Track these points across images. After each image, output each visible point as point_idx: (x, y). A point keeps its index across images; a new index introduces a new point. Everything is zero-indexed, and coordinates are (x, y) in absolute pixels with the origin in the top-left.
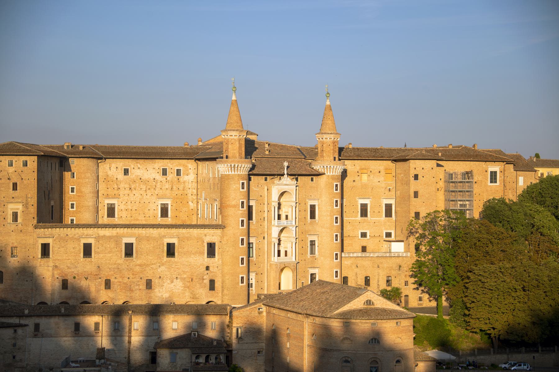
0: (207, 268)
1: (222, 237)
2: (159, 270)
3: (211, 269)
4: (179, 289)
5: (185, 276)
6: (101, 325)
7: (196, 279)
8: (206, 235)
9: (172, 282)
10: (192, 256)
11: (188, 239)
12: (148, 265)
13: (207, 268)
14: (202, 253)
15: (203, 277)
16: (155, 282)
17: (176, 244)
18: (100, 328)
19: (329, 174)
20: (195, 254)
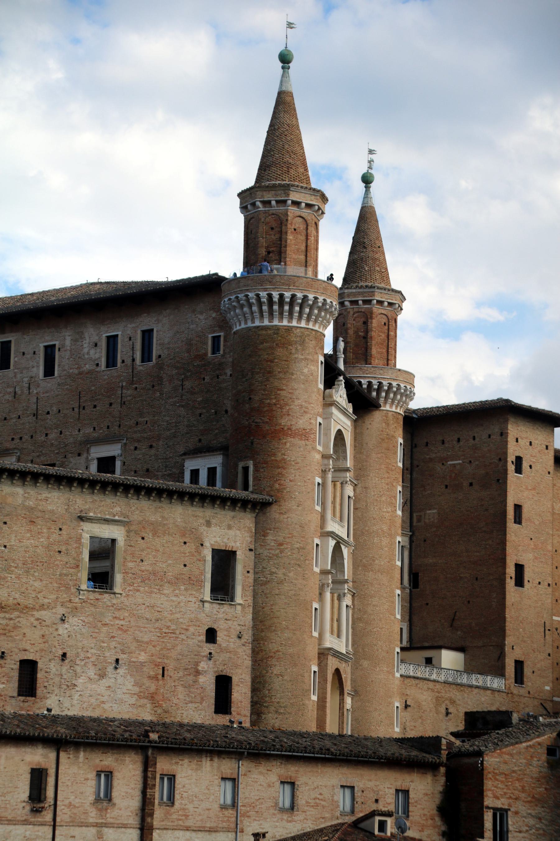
0: (211, 635)
1: (260, 533)
2: (63, 630)
3: (220, 637)
4: (122, 701)
5: (143, 657)
6: (51, 781)
7: (176, 669)
8: (208, 524)
9: (102, 675)
10: (167, 590)
11: (157, 529)
12: (25, 609)
13: (211, 635)
14: (194, 582)
15: (197, 664)
16: (49, 671)
17: (121, 543)
18: (50, 792)
19: (388, 407)
20: (175, 582)
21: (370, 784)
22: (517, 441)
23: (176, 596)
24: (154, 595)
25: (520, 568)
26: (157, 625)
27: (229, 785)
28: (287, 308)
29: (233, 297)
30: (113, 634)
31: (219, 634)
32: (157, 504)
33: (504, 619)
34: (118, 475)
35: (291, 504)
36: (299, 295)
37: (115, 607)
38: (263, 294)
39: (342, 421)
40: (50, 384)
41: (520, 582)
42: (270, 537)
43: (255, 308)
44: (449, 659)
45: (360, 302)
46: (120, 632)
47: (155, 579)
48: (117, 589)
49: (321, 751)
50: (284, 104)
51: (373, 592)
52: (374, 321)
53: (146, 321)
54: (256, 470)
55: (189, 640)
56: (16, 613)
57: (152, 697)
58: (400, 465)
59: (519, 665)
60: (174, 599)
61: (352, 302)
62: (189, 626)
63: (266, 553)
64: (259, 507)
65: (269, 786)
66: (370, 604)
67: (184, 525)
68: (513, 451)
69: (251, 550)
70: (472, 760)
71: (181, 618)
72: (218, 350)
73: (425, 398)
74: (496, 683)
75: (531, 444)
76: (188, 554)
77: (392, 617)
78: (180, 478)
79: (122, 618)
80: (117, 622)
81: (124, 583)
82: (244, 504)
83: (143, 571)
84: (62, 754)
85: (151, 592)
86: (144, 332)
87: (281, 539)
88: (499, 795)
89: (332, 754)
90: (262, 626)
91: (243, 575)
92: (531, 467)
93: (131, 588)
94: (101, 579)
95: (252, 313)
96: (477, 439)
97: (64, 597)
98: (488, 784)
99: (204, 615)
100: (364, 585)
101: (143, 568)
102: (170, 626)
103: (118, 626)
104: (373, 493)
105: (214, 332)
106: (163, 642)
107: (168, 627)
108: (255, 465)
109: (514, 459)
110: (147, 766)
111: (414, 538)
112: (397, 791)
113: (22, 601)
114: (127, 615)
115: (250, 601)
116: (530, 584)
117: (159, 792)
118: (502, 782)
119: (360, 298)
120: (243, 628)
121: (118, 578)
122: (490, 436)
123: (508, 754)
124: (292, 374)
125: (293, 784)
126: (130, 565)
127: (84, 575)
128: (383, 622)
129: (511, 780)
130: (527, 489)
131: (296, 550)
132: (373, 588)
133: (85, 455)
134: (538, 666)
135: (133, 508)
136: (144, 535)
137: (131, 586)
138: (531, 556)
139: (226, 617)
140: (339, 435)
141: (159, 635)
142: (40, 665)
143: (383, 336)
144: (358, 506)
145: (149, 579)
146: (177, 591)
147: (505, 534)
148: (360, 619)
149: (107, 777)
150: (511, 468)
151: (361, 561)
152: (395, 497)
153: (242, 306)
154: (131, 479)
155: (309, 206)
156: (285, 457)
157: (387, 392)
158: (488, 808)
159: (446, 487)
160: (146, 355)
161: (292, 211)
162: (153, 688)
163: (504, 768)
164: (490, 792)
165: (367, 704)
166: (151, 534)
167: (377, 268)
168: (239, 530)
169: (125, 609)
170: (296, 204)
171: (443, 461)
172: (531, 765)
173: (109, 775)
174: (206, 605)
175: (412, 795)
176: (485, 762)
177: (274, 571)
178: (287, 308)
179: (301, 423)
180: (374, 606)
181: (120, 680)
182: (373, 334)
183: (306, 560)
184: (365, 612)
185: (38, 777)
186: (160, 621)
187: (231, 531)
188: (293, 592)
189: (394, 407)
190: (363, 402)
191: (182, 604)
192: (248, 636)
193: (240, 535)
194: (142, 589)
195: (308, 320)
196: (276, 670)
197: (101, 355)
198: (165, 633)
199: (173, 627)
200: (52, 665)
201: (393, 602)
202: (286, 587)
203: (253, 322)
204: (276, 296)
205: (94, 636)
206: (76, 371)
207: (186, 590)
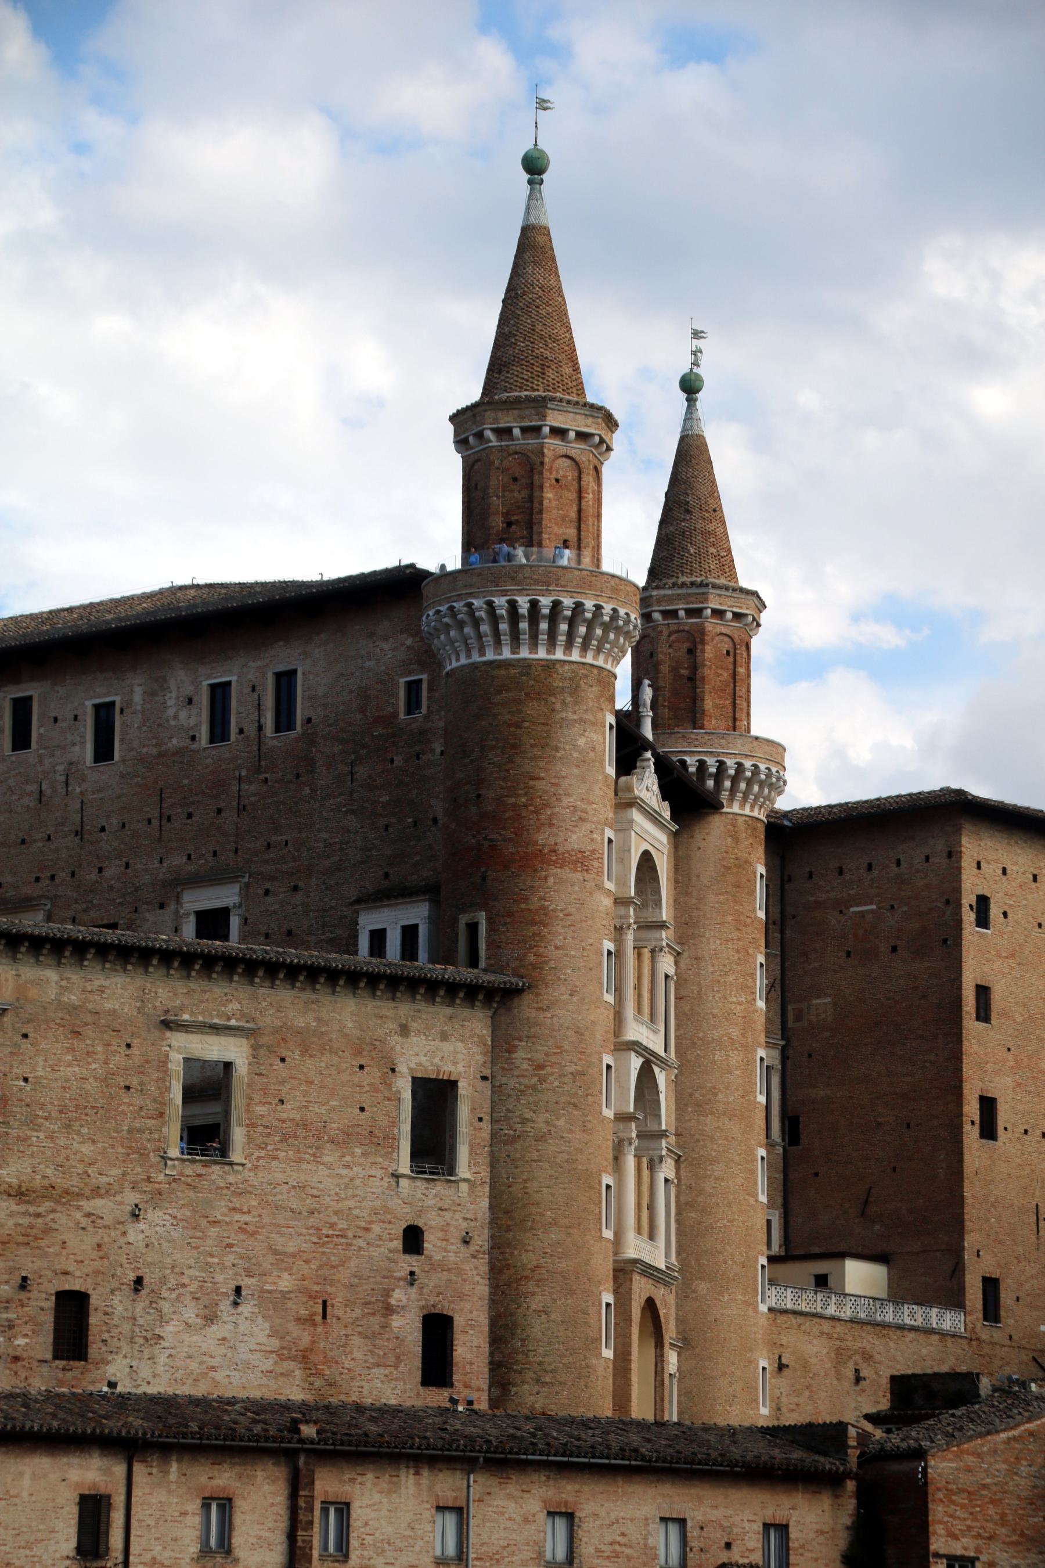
0: (413, 1239)
1: (501, 1047)
2: (135, 1233)
4: (248, 1366)
5: (286, 1282)
6: (117, 1518)
7: (348, 1304)
8: (404, 1031)
9: (210, 1318)
12: (64, 1197)
13: (413, 1239)
15: (387, 1293)
16: (111, 1310)
18: (116, 1540)
19: (736, 808)
20: (344, 1141)
21: (716, 1514)
22: (979, 867)
23: (347, 1166)
24: (304, 1166)
25: (988, 1105)
26: (311, 1221)
27: (451, 1520)
28: (544, 626)
29: (443, 609)
30: (230, 1241)
31: (427, 1236)
32: (308, 995)
33: (961, 1200)
34: (234, 943)
35: (559, 992)
36: (568, 602)
37: (232, 1189)
38: (500, 601)
39: (650, 835)
40: (106, 775)
41: (988, 1130)
42: (520, 1054)
43: (485, 628)
44: (860, 1276)
45: (682, 613)
46: (242, 1237)
47: (307, 1136)
48: (236, 1156)
49: (622, 1453)
50: (533, 249)
51: (714, 1154)
52: (708, 648)
53: (283, 656)
54: (492, 929)
55: (371, 1249)
56: (48, 1204)
57: (304, 1357)
58: (762, 915)
59: (991, 1285)
60: (343, 1172)
61: (666, 614)
62: (371, 1222)
63: (512, 1083)
64: (500, 995)
65: (526, 1520)
66: (710, 1176)
67: (359, 1033)
68: (971, 885)
69: (484, 1078)
70: (905, 1466)
71: (356, 1208)
72: (418, 706)
73: (804, 790)
74: (948, 1320)
75: (1004, 871)
76: (366, 1088)
77: (752, 1201)
78: (350, 945)
79: (245, 1209)
80: (237, 1217)
81: (248, 1144)
82: (471, 994)
83: (284, 1122)
84: (137, 1468)
85: (300, 1160)
86: (279, 676)
87: (540, 1057)
88: (957, 1532)
89: (643, 1458)
90: (508, 1219)
91: (471, 1124)
92: (1005, 914)
93: (263, 1153)
94: (206, 1138)
95: (480, 636)
96: (904, 865)
97: (138, 1171)
98: (937, 1511)
99: (400, 1201)
100: (698, 1141)
101: (284, 1116)
102: (335, 1224)
103: (239, 1224)
104: (711, 969)
105: (410, 673)
106: (323, 1253)
107: (332, 1226)
108: (490, 920)
109: (973, 900)
110: (297, 1487)
111: (790, 1052)
112: (767, 1526)
113: (59, 1181)
114: (255, 1203)
115: (485, 1173)
116: (1009, 1134)
117: (320, 1536)
118: (963, 1506)
119: (681, 606)
120: (473, 1224)
121: (238, 1135)
122: (927, 859)
123: (973, 1454)
124: (557, 749)
125: (570, 1516)
126: (260, 1110)
127: (174, 1131)
128: (734, 1209)
129: (979, 1503)
130: (998, 956)
131: (570, 1076)
132: (715, 1147)
133: (172, 907)
134: (1027, 1287)
135: (264, 1004)
136: (285, 1053)
137: (263, 1149)
138: (1009, 1081)
139: (439, 1205)
140: (646, 858)
141: (316, 1240)
142: (94, 1301)
143: (726, 675)
144: (683, 992)
145: (295, 1137)
146: (348, 1158)
147: (959, 1040)
148: (690, 1205)
149: (222, 1508)
150: (969, 917)
151: (691, 1095)
152: (753, 975)
153: (461, 625)
154: (259, 950)
155: (582, 436)
156: (547, 903)
157: (735, 780)
158: (937, 1555)
159: (848, 954)
160: (284, 719)
161: (552, 445)
162: (306, 1340)
163: (965, 1480)
164: (942, 1526)
165: (707, 1363)
166: (297, 1052)
167: (712, 550)
168: (462, 1041)
169: (250, 1193)
170: (559, 433)
171: (841, 906)
172: (1016, 1474)
173: (226, 1504)
174: (404, 1182)
175: (794, 1533)
176: (929, 1470)
177: (527, 1116)
178: (544, 626)
179: (575, 840)
180: (717, 1179)
181: (244, 1326)
182: (706, 671)
183: (587, 1095)
184: (701, 1192)
185: (93, 1511)
186: (316, 1215)
187: (445, 1044)
188: (565, 1156)
189: (748, 807)
190: (690, 800)
191: (358, 1182)
192: (481, 1240)
193: (465, 1051)
194: (282, 1154)
195: (585, 647)
196: (536, 1303)
197: (199, 719)
198: (327, 1236)
199: (342, 1225)
200: (116, 1299)
201: (753, 1172)
202: (551, 1146)
203: (482, 653)
204: (523, 603)
205: (193, 1245)
206: (154, 751)
207: (365, 1154)
